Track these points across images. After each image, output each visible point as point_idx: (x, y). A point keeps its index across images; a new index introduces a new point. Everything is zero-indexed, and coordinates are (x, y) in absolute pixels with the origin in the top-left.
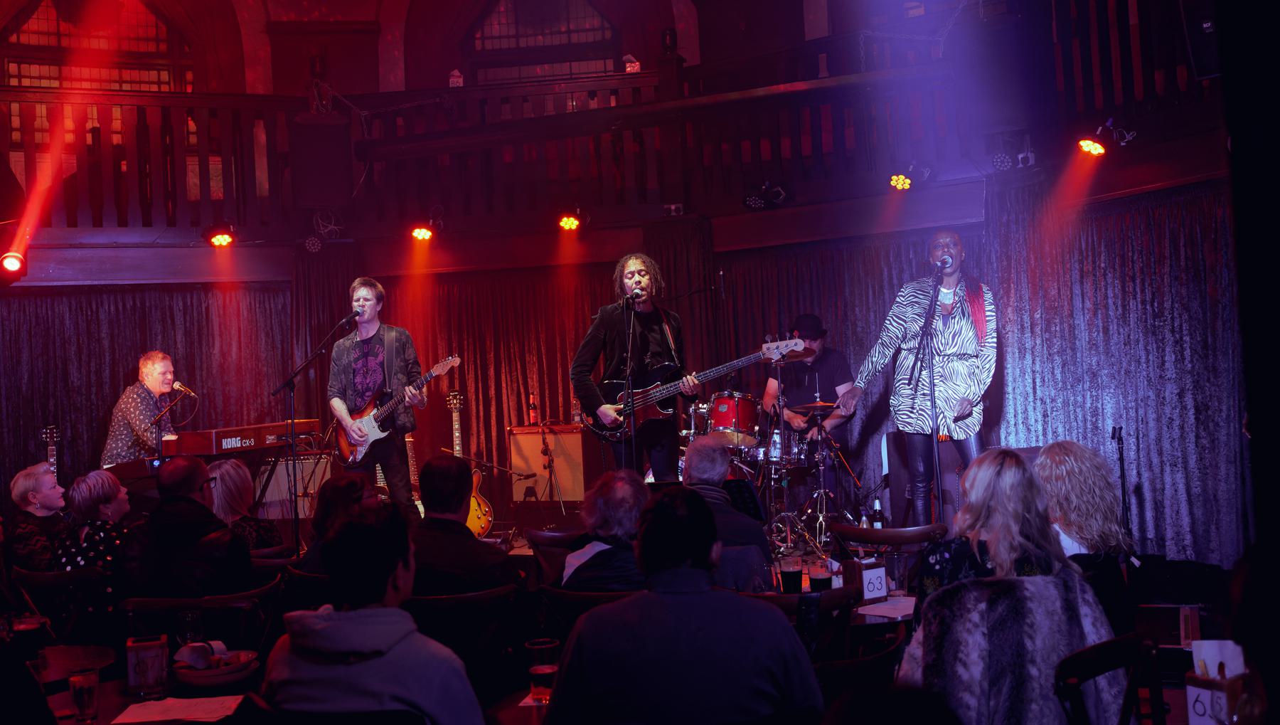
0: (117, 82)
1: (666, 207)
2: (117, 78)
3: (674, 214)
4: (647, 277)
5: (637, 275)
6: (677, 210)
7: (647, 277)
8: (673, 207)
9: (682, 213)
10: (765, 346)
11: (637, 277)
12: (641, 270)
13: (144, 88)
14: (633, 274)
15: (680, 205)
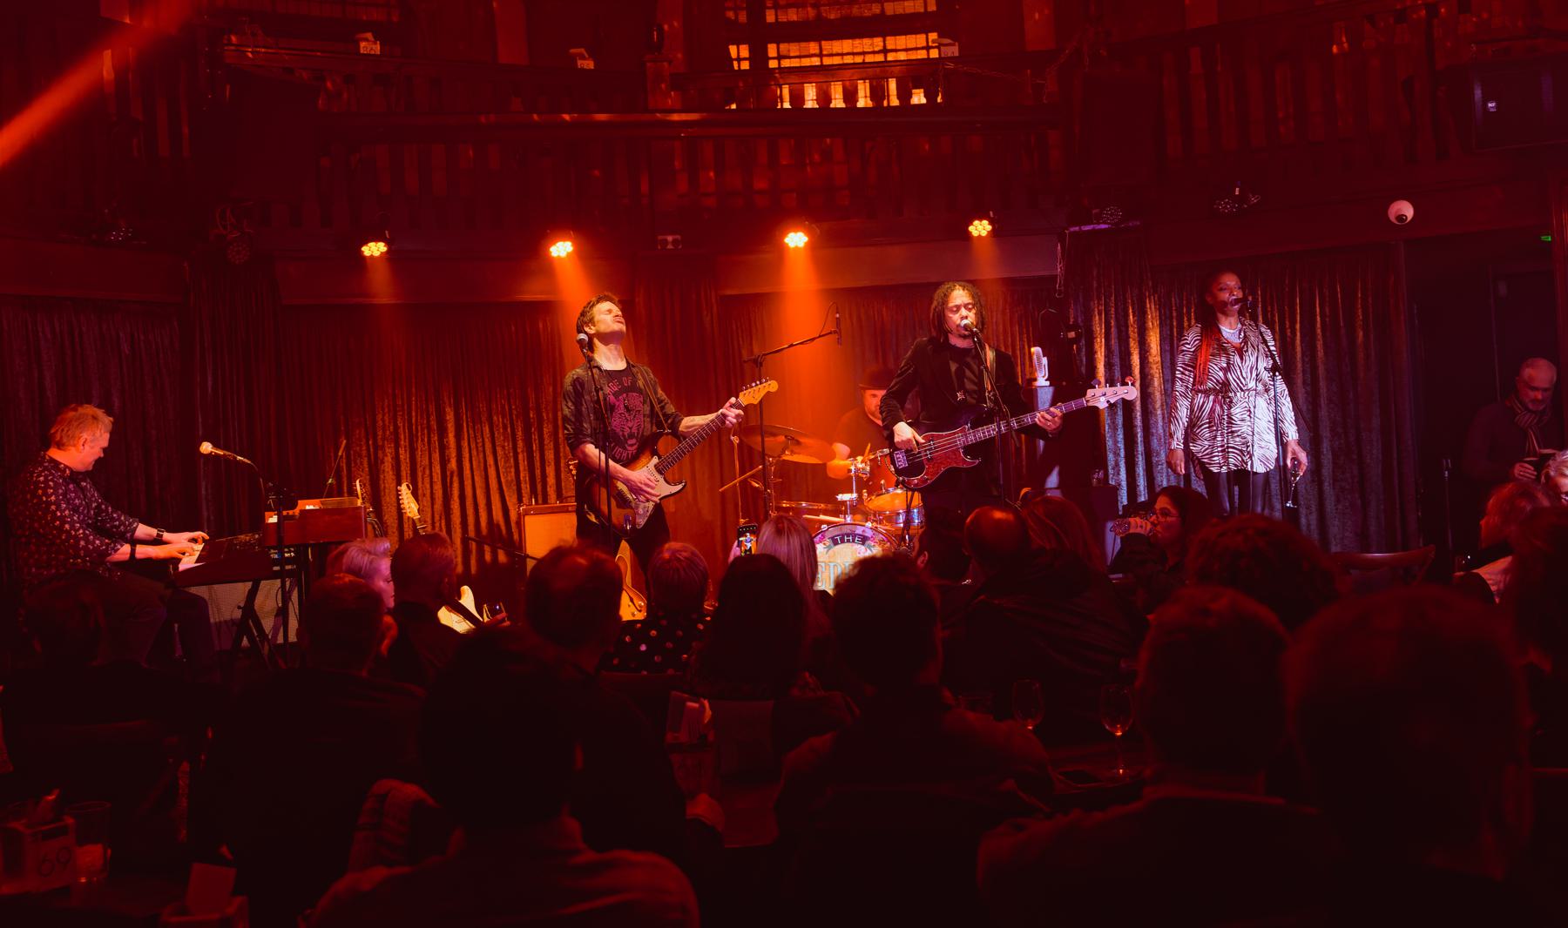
0: (923, 48)
1: (660, 237)
2: (924, 44)
3: (670, 247)
4: (974, 311)
5: (963, 309)
6: (675, 242)
7: (974, 311)
8: (670, 238)
9: (680, 247)
10: (1090, 392)
11: (964, 312)
12: (969, 304)
13: (869, 59)
14: (958, 308)
15: (678, 237)
